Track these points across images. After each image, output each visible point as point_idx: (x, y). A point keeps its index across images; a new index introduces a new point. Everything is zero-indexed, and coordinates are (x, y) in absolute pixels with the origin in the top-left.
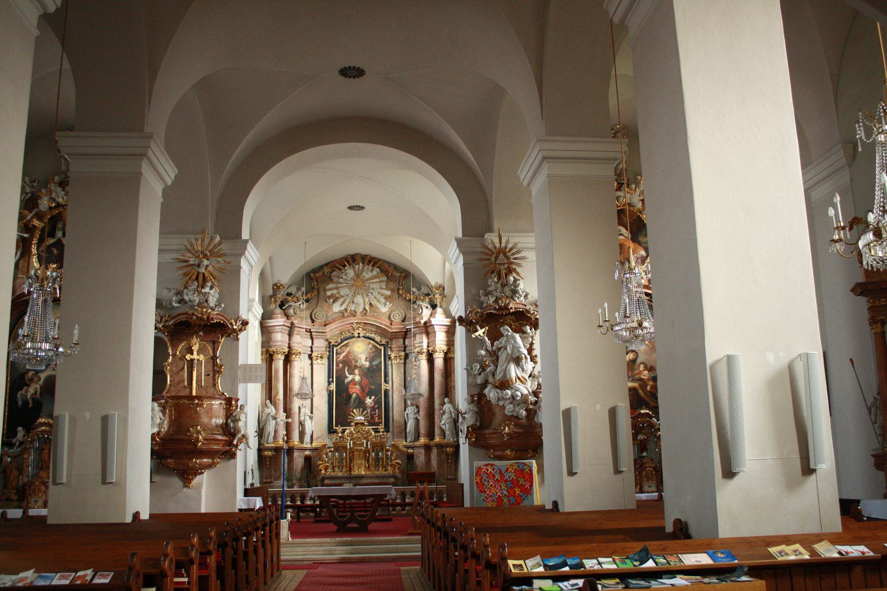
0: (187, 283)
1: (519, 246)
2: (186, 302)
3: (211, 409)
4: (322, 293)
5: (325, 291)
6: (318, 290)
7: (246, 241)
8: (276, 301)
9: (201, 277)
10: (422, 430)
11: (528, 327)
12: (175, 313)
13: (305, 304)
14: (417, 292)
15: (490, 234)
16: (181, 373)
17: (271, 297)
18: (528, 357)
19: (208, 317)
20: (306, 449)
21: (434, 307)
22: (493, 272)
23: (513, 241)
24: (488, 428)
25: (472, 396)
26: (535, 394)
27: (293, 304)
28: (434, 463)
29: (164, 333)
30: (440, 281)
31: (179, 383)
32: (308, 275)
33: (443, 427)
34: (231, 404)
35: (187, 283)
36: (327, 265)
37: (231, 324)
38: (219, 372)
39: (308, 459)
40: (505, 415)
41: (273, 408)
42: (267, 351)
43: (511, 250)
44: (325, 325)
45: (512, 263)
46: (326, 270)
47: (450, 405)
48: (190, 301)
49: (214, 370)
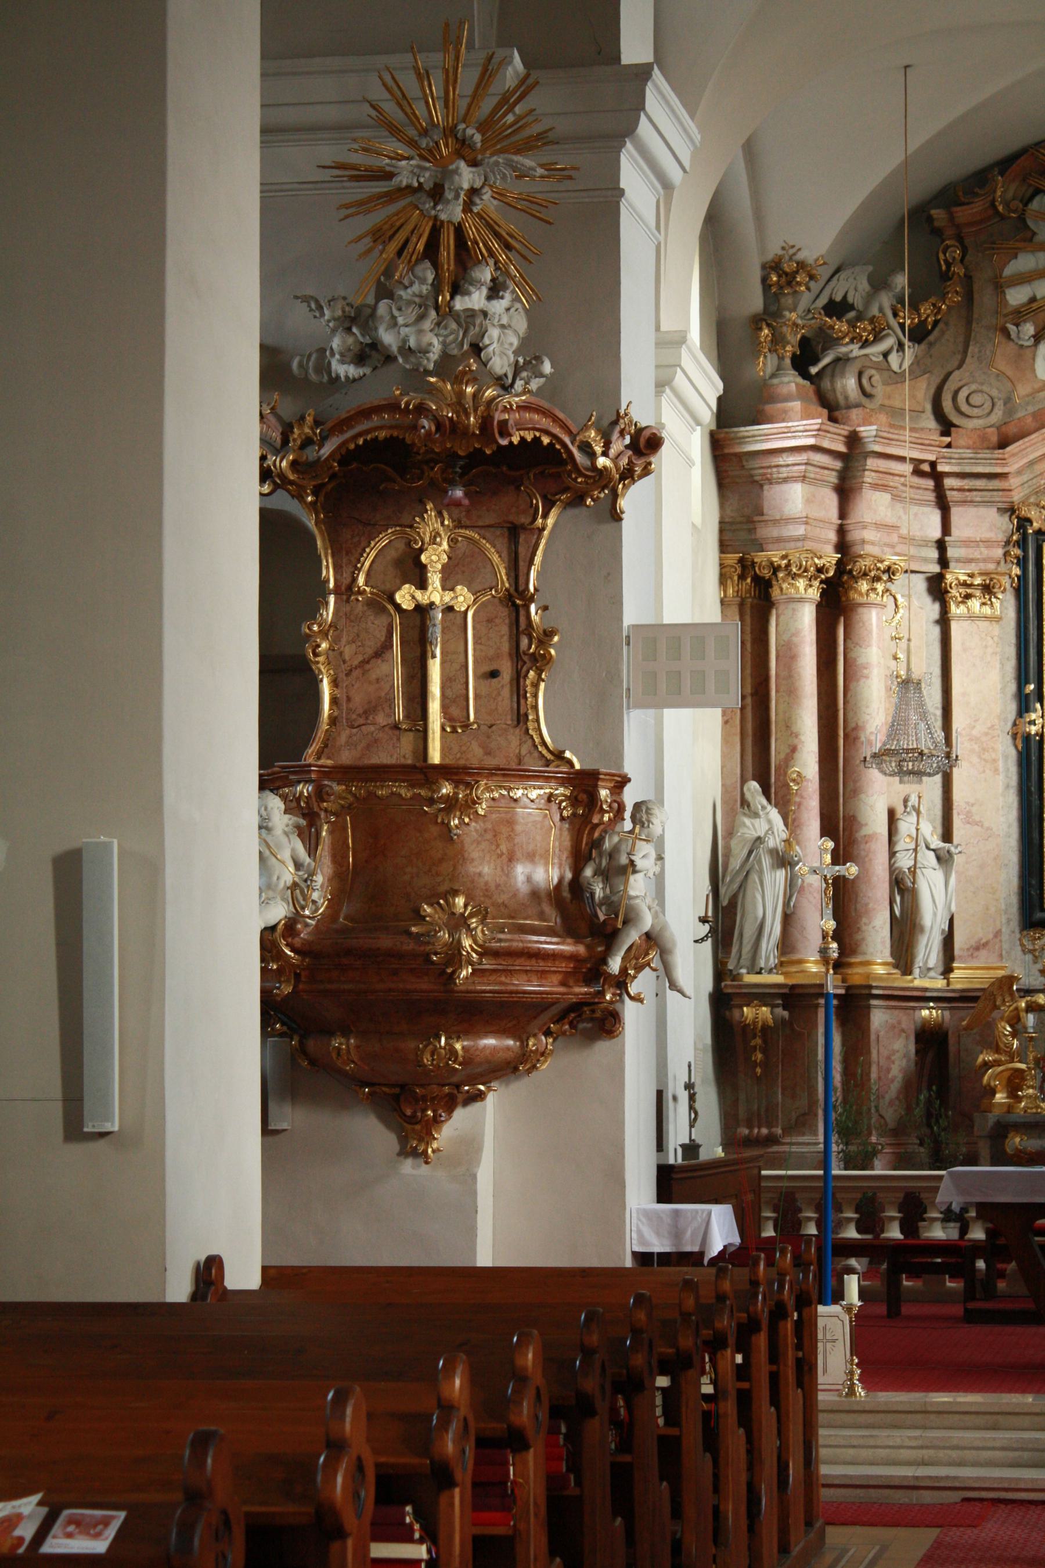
0: (388, 273)
2: (390, 359)
3: (511, 822)
4: (985, 298)
5: (999, 286)
6: (968, 278)
7: (642, 73)
8: (777, 340)
9: (448, 240)
12: (345, 404)
13: (910, 352)
16: (379, 668)
17: (756, 322)
19: (486, 422)
20: (922, 998)
27: (855, 350)
29: (301, 498)
31: (369, 711)
32: (919, 215)
34: (592, 802)
35: (388, 273)
36: (1005, 164)
37: (586, 448)
38: (540, 662)
39: (931, 1041)
41: (774, 814)
42: (746, 566)
44: (1003, 444)
46: (1004, 190)
48: (407, 351)
49: (516, 654)
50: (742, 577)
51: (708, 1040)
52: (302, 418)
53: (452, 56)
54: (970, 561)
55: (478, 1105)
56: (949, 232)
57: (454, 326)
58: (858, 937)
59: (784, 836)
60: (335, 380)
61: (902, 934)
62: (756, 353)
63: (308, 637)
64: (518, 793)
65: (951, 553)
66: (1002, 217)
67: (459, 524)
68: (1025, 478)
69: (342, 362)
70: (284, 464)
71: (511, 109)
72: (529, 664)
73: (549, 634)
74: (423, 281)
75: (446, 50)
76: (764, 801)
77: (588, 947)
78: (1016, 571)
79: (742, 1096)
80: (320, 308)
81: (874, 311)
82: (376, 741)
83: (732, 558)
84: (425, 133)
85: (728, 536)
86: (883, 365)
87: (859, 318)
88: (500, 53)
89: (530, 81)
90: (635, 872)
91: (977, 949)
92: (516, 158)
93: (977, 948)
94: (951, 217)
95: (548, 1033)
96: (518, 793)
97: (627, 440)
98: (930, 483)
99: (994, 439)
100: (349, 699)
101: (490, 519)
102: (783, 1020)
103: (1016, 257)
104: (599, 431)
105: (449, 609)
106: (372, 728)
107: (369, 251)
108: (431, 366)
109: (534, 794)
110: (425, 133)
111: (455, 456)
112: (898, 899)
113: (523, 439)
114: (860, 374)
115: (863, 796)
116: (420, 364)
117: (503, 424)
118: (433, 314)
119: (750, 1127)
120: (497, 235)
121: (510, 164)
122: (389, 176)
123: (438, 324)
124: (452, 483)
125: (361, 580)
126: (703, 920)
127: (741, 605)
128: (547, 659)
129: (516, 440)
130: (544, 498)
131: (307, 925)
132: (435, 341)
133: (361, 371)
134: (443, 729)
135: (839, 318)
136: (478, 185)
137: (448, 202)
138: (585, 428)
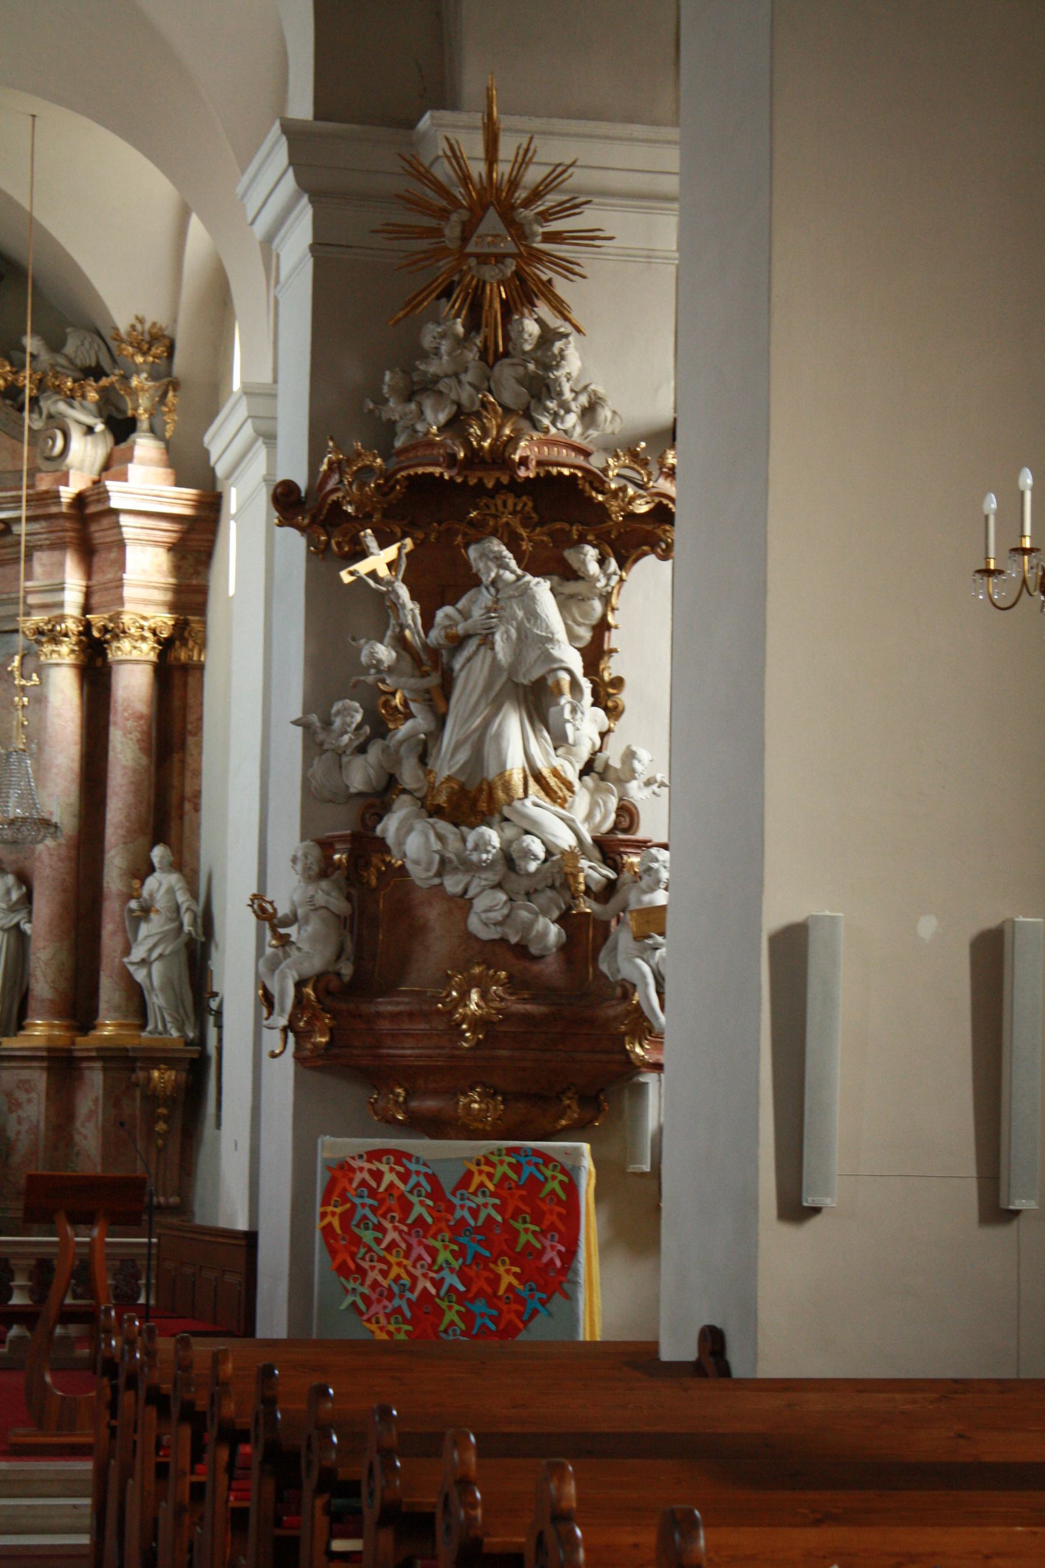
1: (578, 178)
10: (43, 985)
11: (591, 553)
14: (45, 357)
15: (447, 116)
18: (586, 685)
21: (122, 428)
22: (447, 293)
23: (551, 152)
24: (389, 989)
25: (326, 846)
26: (608, 848)
28: (89, 1136)
30: (155, 315)
33: (140, 975)
40: (470, 937)
43: (536, 195)
45: (538, 257)
47: (174, 879)
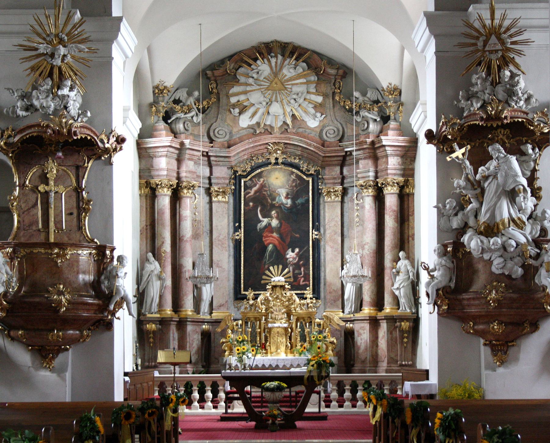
0: (36, 82)
1: (521, 23)
2: (37, 110)
3: (78, 261)
4: (223, 100)
5: (228, 96)
6: (218, 94)
7: (120, 19)
8: (158, 111)
9: (56, 71)
10: (367, 297)
11: (530, 146)
12: (22, 124)
13: (201, 116)
14: (361, 99)
15: (477, 6)
16: (33, 211)
17: (151, 105)
18: (529, 190)
19: (69, 131)
20: (203, 322)
21: (385, 119)
22: (479, 64)
23: (512, 15)
24: (466, 291)
25: (445, 246)
26: (538, 243)
27: (182, 115)
28: (383, 343)
29: (7, 155)
30: (395, 82)
31: (31, 225)
32: (204, 72)
33: (397, 293)
34: (104, 254)
35: (36, 82)
36: (230, 57)
37: (102, 141)
38: (86, 210)
39: (206, 336)
40: (492, 273)
41: (157, 263)
42: (148, 184)
43: (508, 29)
44: (229, 147)
45: (509, 50)
46: (230, 66)
47: (407, 262)
48: (43, 107)
49: (79, 208)
50: (146, 187)
51: (136, 335)
52: (8, 129)
53: (57, 10)
54: (218, 184)
55: (66, 353)
56: (213, 78)
57: (58, 99)
58: (183, 302)
59: (160, 270)
60: (18, 116)
61: (197, 302)
62: (151, 115)
63: (10, 200)
64: (80, 252)
65: (213, 181)
66: (229, 75)
67: (59, 165)
68: (236, 158)
69: (21, 110)
70: (2, 143)
71: (76, 30)
72: (83, 211)
73: (89, 201)
74: (48, 85)
75: (55, 9)
76: (154, 259)
77: (103, 302)
78: (233, 187)
79: (146, 353)
80: (13, 92)
81: (189, 103)
82: (33, 235)
83: (143, 181)
84: (48, 35)
85: (142, 174)
86: (191, 121)
87: (184, 105)
88: (73, 11)
89: (83, 20)
90: (118, 277)
91: (220, 306)
92: (79, 45)
93: (220, 306)
94: (213, 74)
95: (89, 329)
96: (80, 252)
97: (115, 139)
98: (206, 159)
99: (226, 145)
100: (23, 221)
101: (70, 163)
102: (159, 328)
103: (233, 87)
104: (106, 136)
105: (56, 193)
106: (31, 231)
107: (29, 74)
108: (51, 113)
109: (85, 252)
110: (48, 35)
111: (59, 142)
112: (196, 290)
113: (81, 137)
114: (184, 123)
115: (185, 258)
116: (47, 112)
117: (75, 132)
118: (51, 95)
119: (149, 362)
120: (72, 70)
121: (77, 47)
122: (36, 49)
123: (53, 99)
124: (58, 151)
125: (27, 182)
126: (135, 296)
127: (146, 196)
128: (89, 209)
129: (79, 137)
130: (88, 157)
131: (10, 294)
132: (52, 105)
133: (27, 114)
134: (55, 231)
135: (178, 105)
136: (66, 54)
137: (56, 59)
138: (101, 134)
